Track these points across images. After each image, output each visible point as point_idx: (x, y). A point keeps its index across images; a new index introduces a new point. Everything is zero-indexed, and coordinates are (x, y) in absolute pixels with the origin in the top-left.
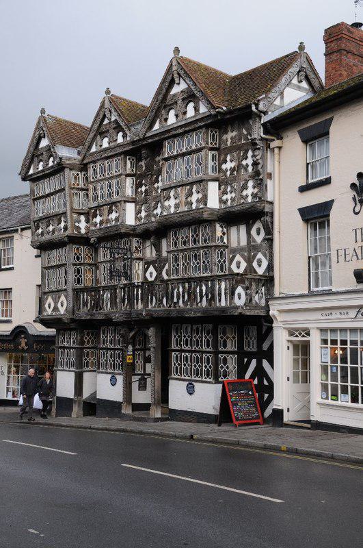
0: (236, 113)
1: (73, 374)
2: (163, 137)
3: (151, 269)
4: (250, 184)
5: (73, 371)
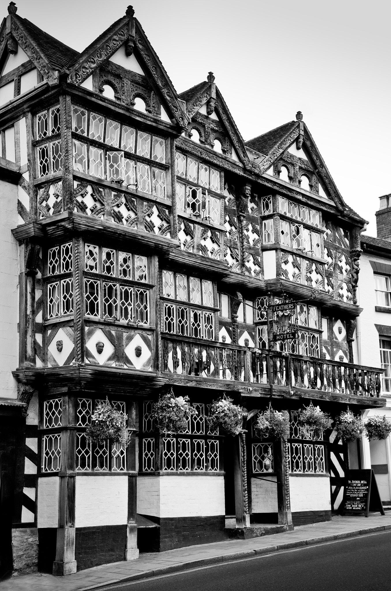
0: (346, 219)
1: (126, 478)
2: (281, 190)
3: (223, 332)
4: (345, 286)
5: (125, 474)
